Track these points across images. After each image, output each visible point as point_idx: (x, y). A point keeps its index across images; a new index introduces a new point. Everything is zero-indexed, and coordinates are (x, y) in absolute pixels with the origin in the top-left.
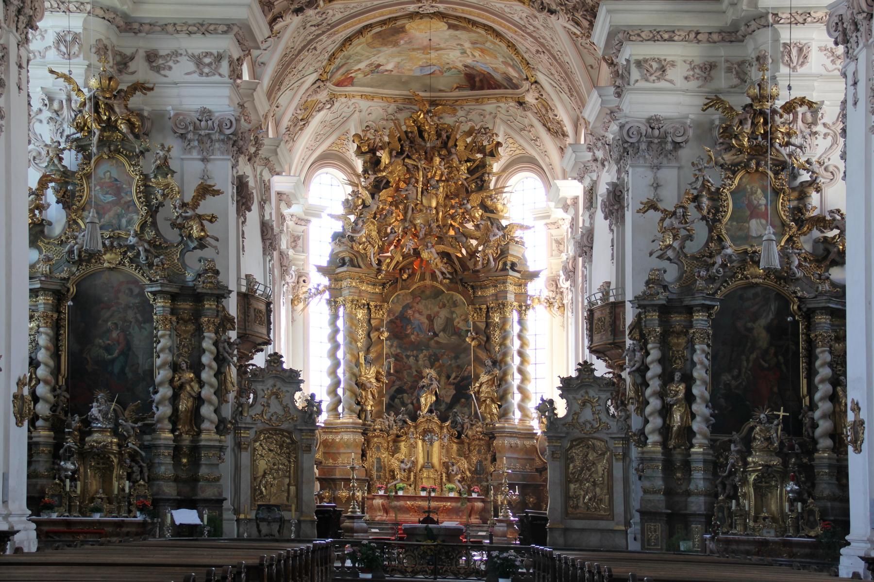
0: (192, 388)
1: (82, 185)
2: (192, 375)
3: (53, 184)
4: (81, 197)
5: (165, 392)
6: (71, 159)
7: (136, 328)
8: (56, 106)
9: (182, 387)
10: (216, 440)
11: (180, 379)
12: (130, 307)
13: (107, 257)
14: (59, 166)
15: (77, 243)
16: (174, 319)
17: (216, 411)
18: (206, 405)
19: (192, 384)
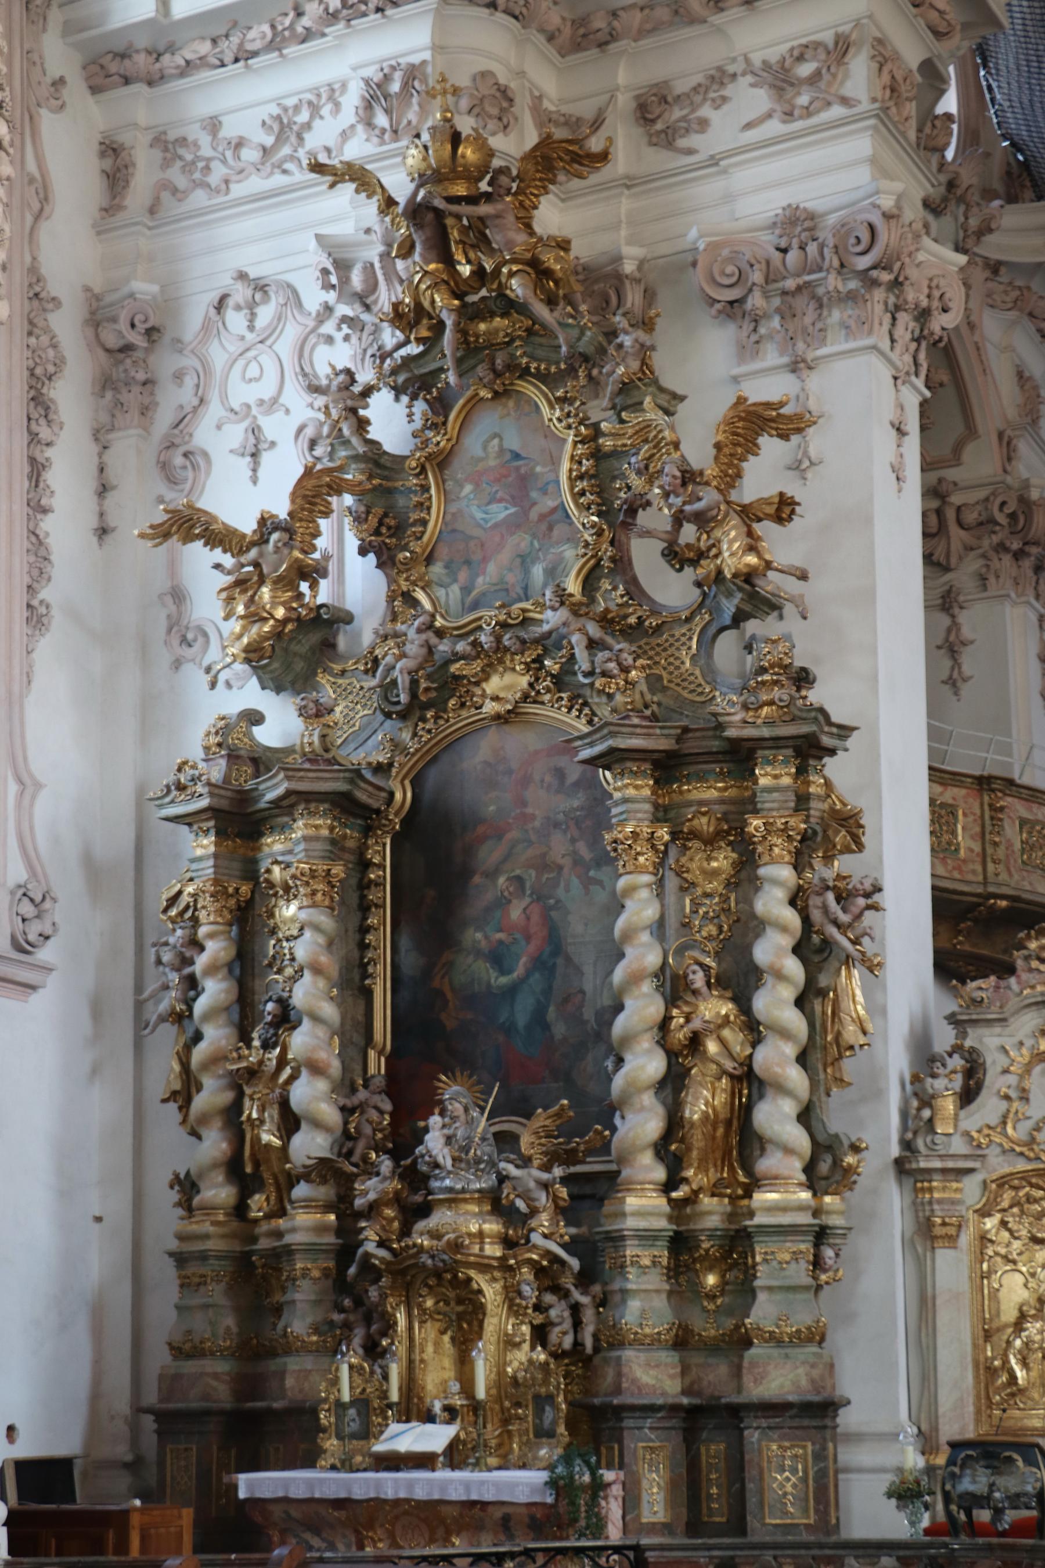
0: (722, 1041)
1: (426, 489)
2: (726, 1008)
3: (348, 500)
4: (424, 523)
5: (646, 1064)
6: (391, 422)
7: (575, 881)
8: (357, 280)
9: (695, 1042)
10: (801, 1208)
11: (688, 1020)
12: (557, 825)
13: (494, 684)
14: (355, 441)
15: (403, 655)
16: (663, 833)
17: (805, 1117)
18: (770, 1093)
19: (726, 1033)
